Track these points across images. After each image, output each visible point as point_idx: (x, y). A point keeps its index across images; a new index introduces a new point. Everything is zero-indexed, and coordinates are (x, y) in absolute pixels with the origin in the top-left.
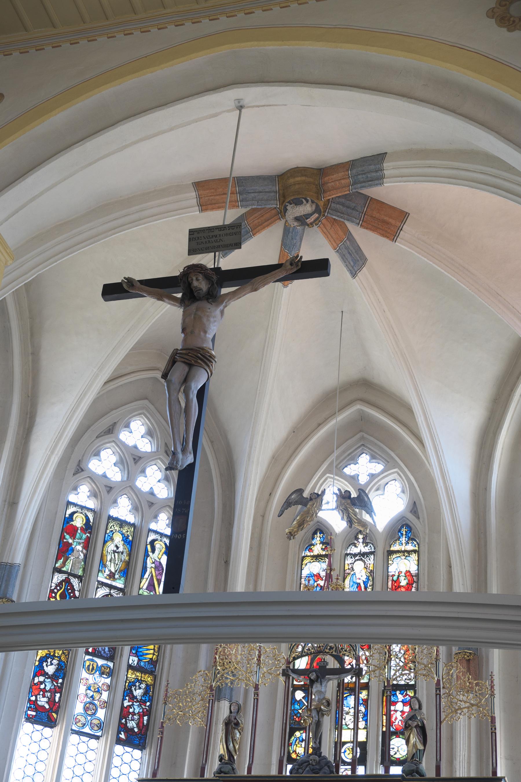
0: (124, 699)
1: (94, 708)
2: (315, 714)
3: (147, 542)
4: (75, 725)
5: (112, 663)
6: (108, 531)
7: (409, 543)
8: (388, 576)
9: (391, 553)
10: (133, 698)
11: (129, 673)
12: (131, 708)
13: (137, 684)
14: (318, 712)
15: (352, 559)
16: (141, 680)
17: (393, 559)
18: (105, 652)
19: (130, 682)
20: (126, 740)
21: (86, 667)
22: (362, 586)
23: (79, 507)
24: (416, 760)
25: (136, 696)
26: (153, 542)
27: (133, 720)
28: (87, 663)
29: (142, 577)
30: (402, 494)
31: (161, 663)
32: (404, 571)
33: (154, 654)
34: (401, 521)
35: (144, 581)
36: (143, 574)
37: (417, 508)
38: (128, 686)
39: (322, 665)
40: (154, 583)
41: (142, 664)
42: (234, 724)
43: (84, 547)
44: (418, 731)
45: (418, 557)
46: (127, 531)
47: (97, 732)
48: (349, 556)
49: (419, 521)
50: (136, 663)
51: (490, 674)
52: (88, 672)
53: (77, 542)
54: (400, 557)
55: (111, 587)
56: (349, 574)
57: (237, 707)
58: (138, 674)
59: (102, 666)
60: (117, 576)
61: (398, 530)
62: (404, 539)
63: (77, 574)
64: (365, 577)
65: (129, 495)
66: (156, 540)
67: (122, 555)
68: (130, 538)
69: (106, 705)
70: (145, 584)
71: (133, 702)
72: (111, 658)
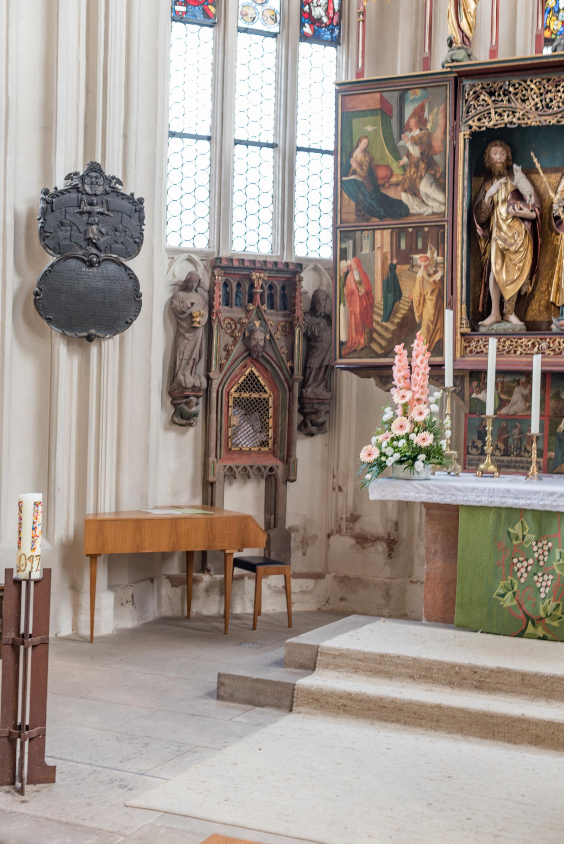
4: (242, 20)
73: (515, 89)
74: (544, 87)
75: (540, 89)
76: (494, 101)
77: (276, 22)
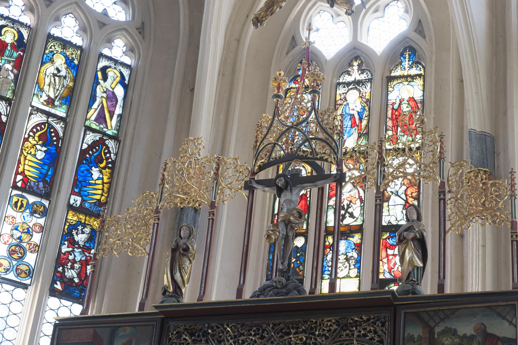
0: (62, 244)
1: (22, 251)
2: (282, 227)
3: (97, 68)
5: (48, 202)
6: (47, 52)
7: (413, 67)
8: (387, 105)
9: (391, 79)
10: (73, 243)
11: (69, 214)
12: (71, 255)
13: (80, 228)
14: (286, 225)
15: (345, 89)
16: (85, 223)
17: (394, 85)
18: (38, 188)
19: (70, 225)
20: (63, 291)
21: (13, 203)
22: (357, 117)
23: (9, 21)
24: (412, 280)
25: (78, 241)
26: (104, 70)
27: (72, 268)
28: (15, 199)
29: (90, 107)
30: (406, 14)
31: (111, 205)
32: (406, 98)
33: (102, 195)
34: (403, 42)
35: (91, 112)
36: (91, 104)
37: (422, 27)
38: (67, 229)
39: (295, 173)
40: (105, 115)
41: (87, 205)
42: (183, 250)
43: (14, 67)
44: (416, 244)
45: (424, 81)
46: (72, 54)
47: (24, 279)
48: (341, 85)
49: (426, 41)
50: (78, 203)
51: (510, 171)
52: (15, 209)
53: (6, 60)
54: (402, 82)
55: (48, 114)
56: (340, 105)
57: (188, 232)
58: (81, 216)
59: (34, 203)
60: (57, 103)
61: (400, 54)
62: (407, 62)
63: (5, 95)
64: (361, 107)
65: (75, 14)
66: (110, 67)
67: (64, 80)
68: (76, 62)
69: (36, 248)
70: (93, 114)
71: (74, 248)
72: (47, 196)
73: (212, 331)
74: (238, 331)
75: (234, 333)
76: (194, 340)
77: (29, 275)
